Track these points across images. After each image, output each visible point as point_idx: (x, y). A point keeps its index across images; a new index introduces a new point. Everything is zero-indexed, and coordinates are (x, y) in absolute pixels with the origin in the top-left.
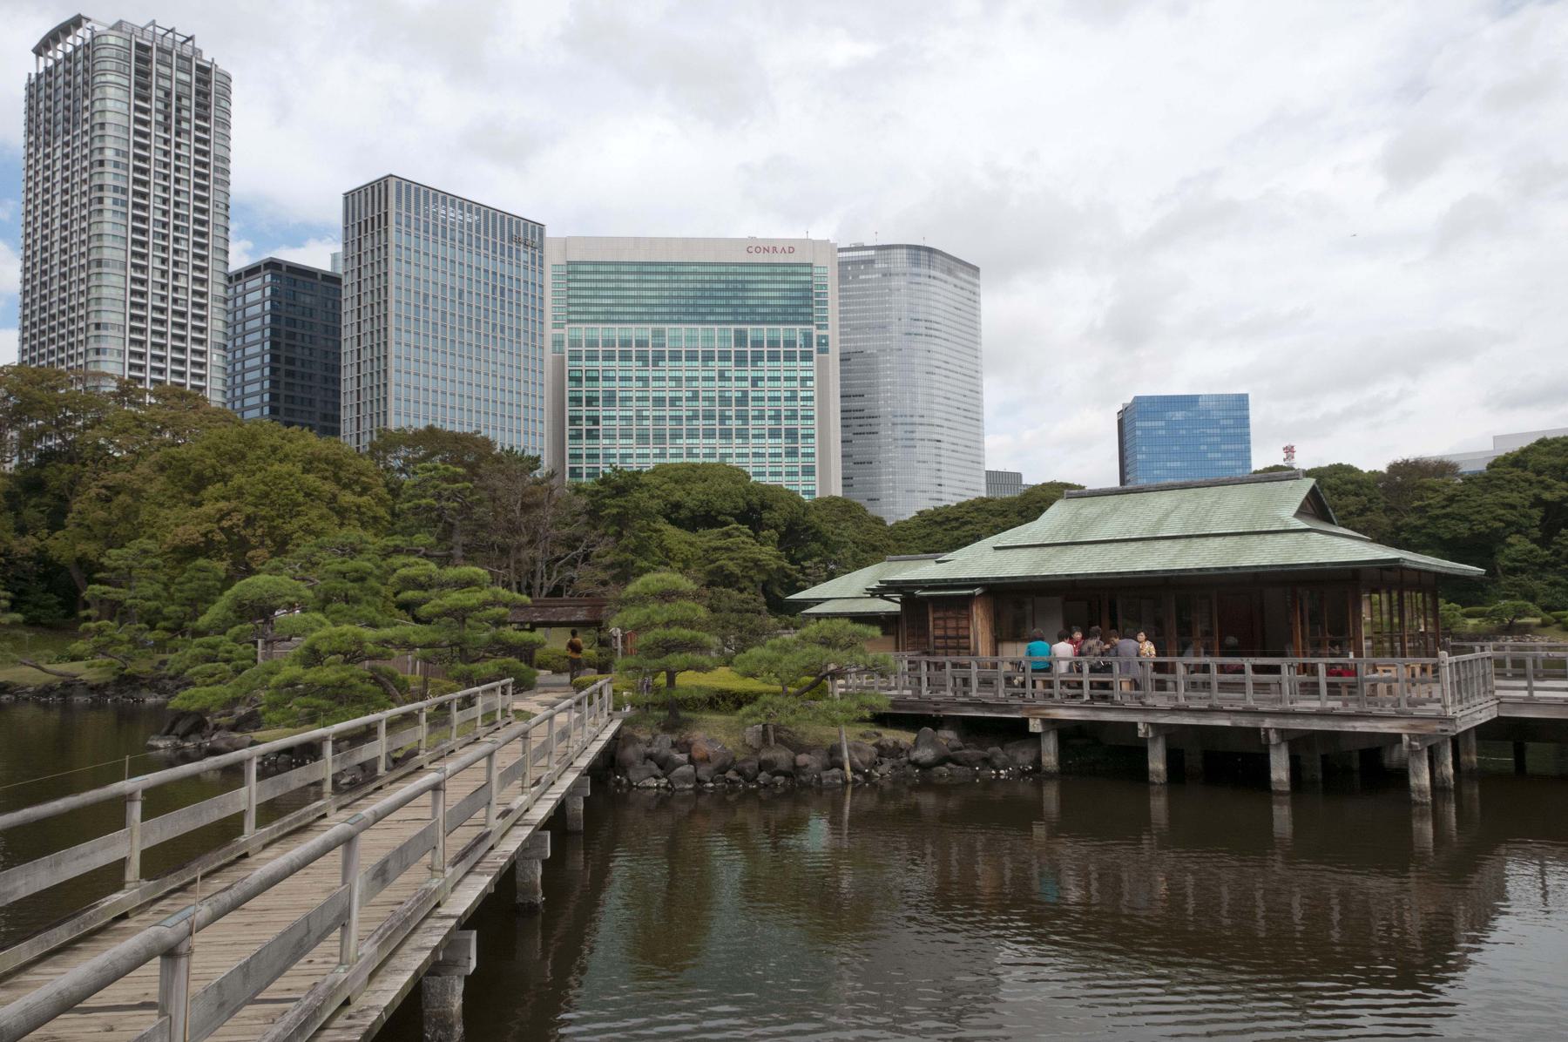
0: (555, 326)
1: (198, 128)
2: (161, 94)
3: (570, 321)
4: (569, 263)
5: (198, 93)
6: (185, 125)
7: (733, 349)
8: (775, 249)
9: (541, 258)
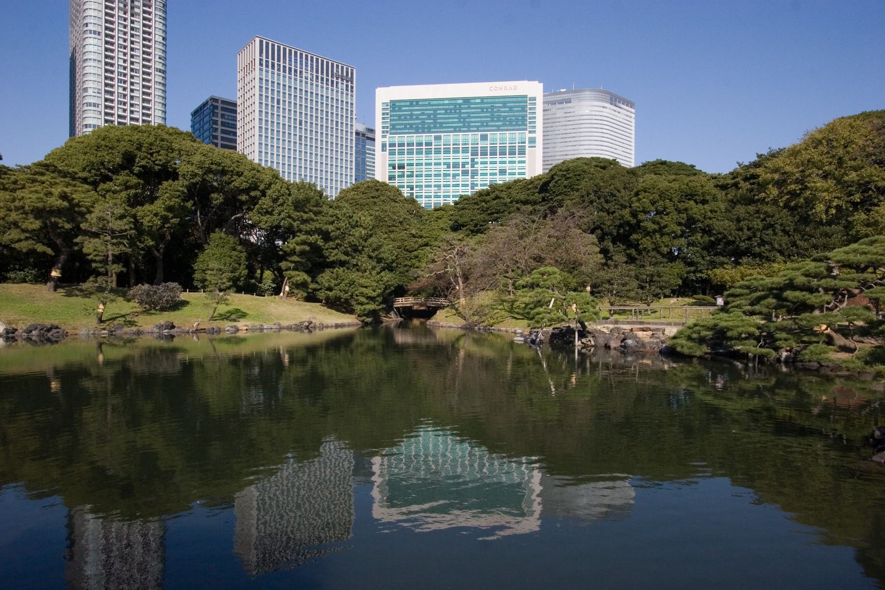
0: (384, 137)
3: (391, 134)
4: (391, 101)
6: (136, 10)
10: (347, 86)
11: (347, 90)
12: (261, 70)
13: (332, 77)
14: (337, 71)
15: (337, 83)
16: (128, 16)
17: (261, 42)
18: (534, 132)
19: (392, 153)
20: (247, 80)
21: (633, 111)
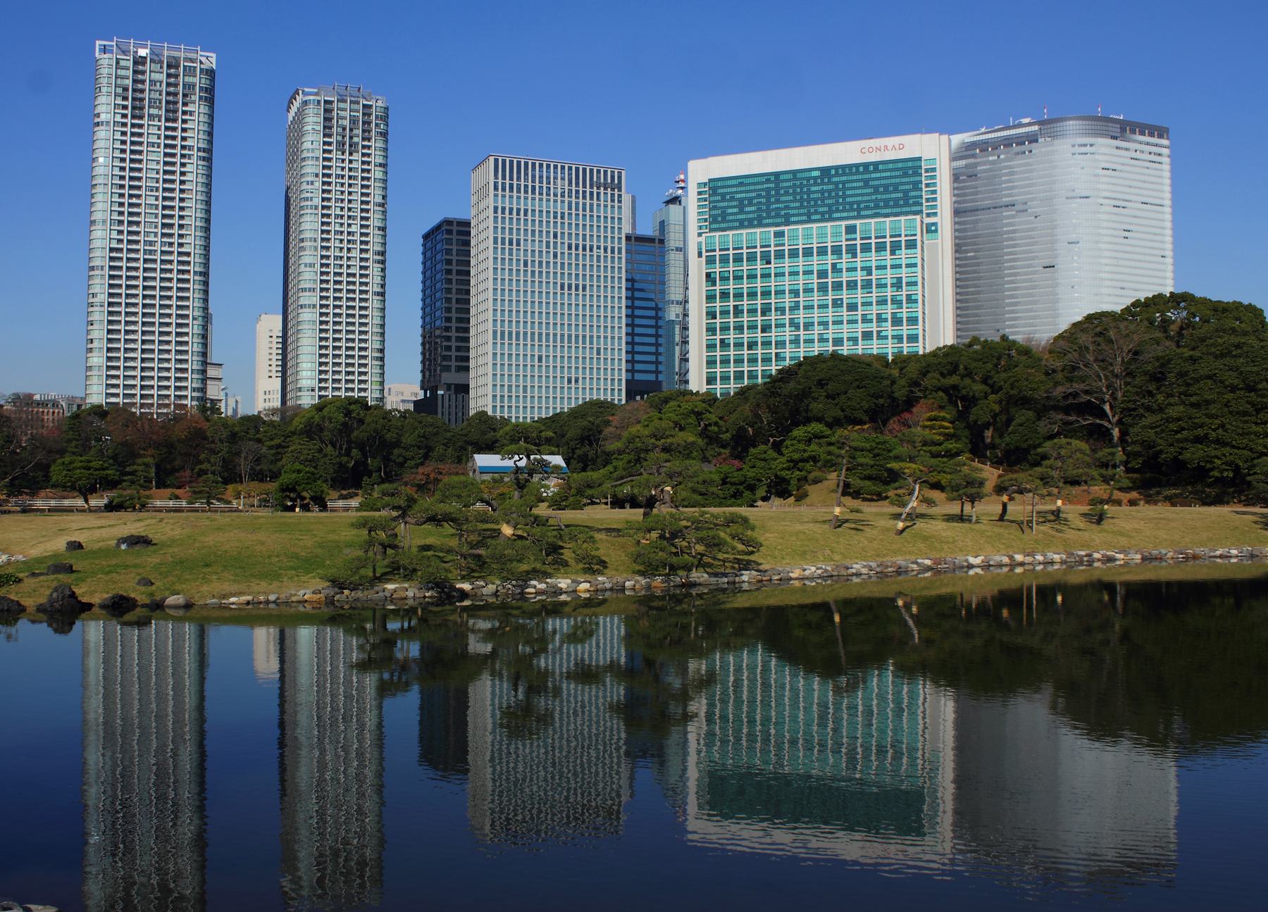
1: (364, 147)
2: (340, 130)
5: (364, 123)
7: (844, 243)
8: (886, 147)
9: (620, 196)
10: (613, 195)
11: (613, 201)
12: (496, 196)
13: (591, 187)
14: (599, 178)
15: (598, 194)
16: (346, 156)
17: (496, 161)
18: (935, 214)
19: (710, 261)
20: (482, 206)
21: (1165, 142)
